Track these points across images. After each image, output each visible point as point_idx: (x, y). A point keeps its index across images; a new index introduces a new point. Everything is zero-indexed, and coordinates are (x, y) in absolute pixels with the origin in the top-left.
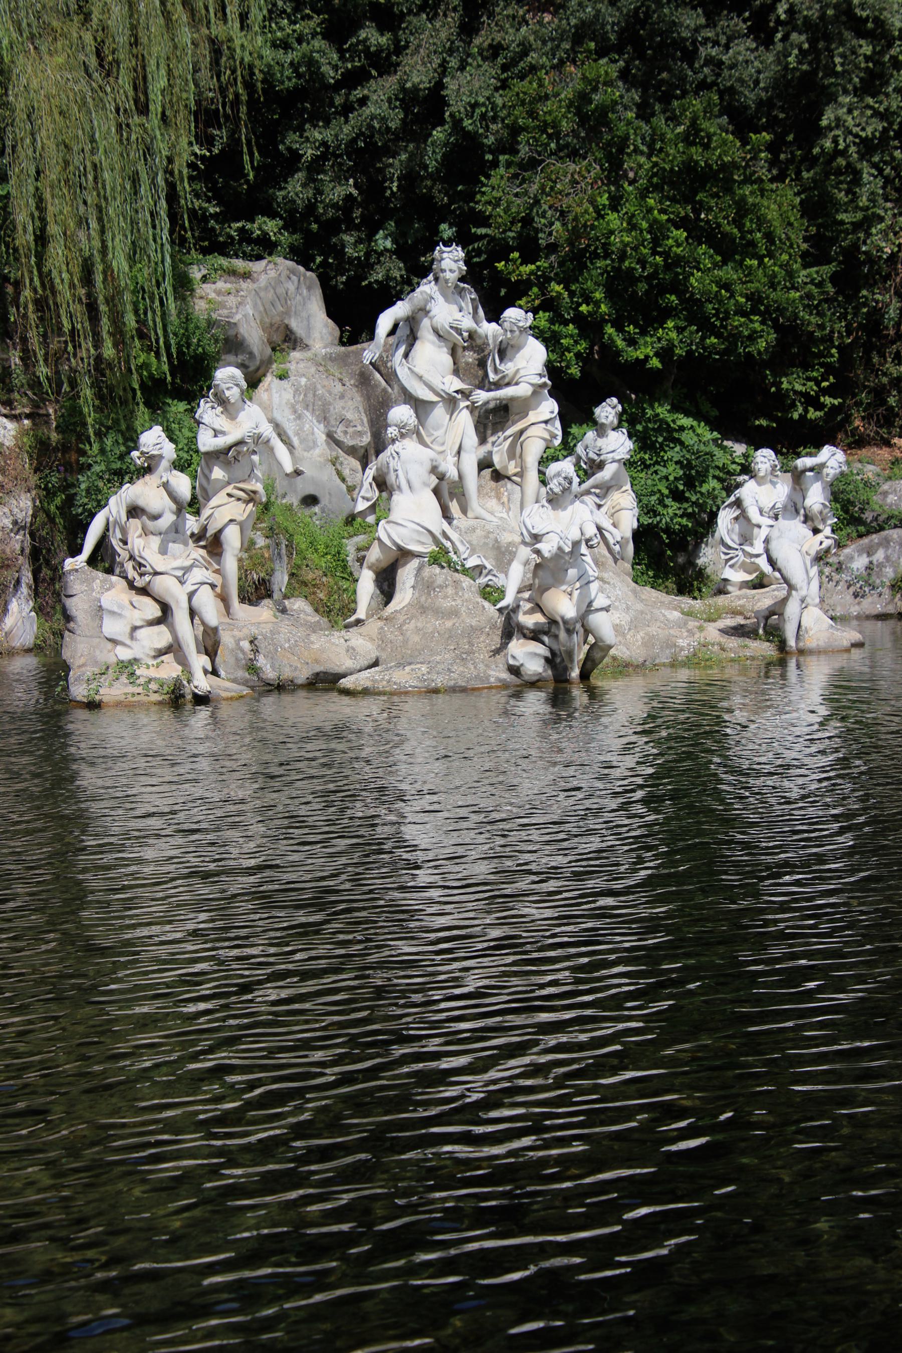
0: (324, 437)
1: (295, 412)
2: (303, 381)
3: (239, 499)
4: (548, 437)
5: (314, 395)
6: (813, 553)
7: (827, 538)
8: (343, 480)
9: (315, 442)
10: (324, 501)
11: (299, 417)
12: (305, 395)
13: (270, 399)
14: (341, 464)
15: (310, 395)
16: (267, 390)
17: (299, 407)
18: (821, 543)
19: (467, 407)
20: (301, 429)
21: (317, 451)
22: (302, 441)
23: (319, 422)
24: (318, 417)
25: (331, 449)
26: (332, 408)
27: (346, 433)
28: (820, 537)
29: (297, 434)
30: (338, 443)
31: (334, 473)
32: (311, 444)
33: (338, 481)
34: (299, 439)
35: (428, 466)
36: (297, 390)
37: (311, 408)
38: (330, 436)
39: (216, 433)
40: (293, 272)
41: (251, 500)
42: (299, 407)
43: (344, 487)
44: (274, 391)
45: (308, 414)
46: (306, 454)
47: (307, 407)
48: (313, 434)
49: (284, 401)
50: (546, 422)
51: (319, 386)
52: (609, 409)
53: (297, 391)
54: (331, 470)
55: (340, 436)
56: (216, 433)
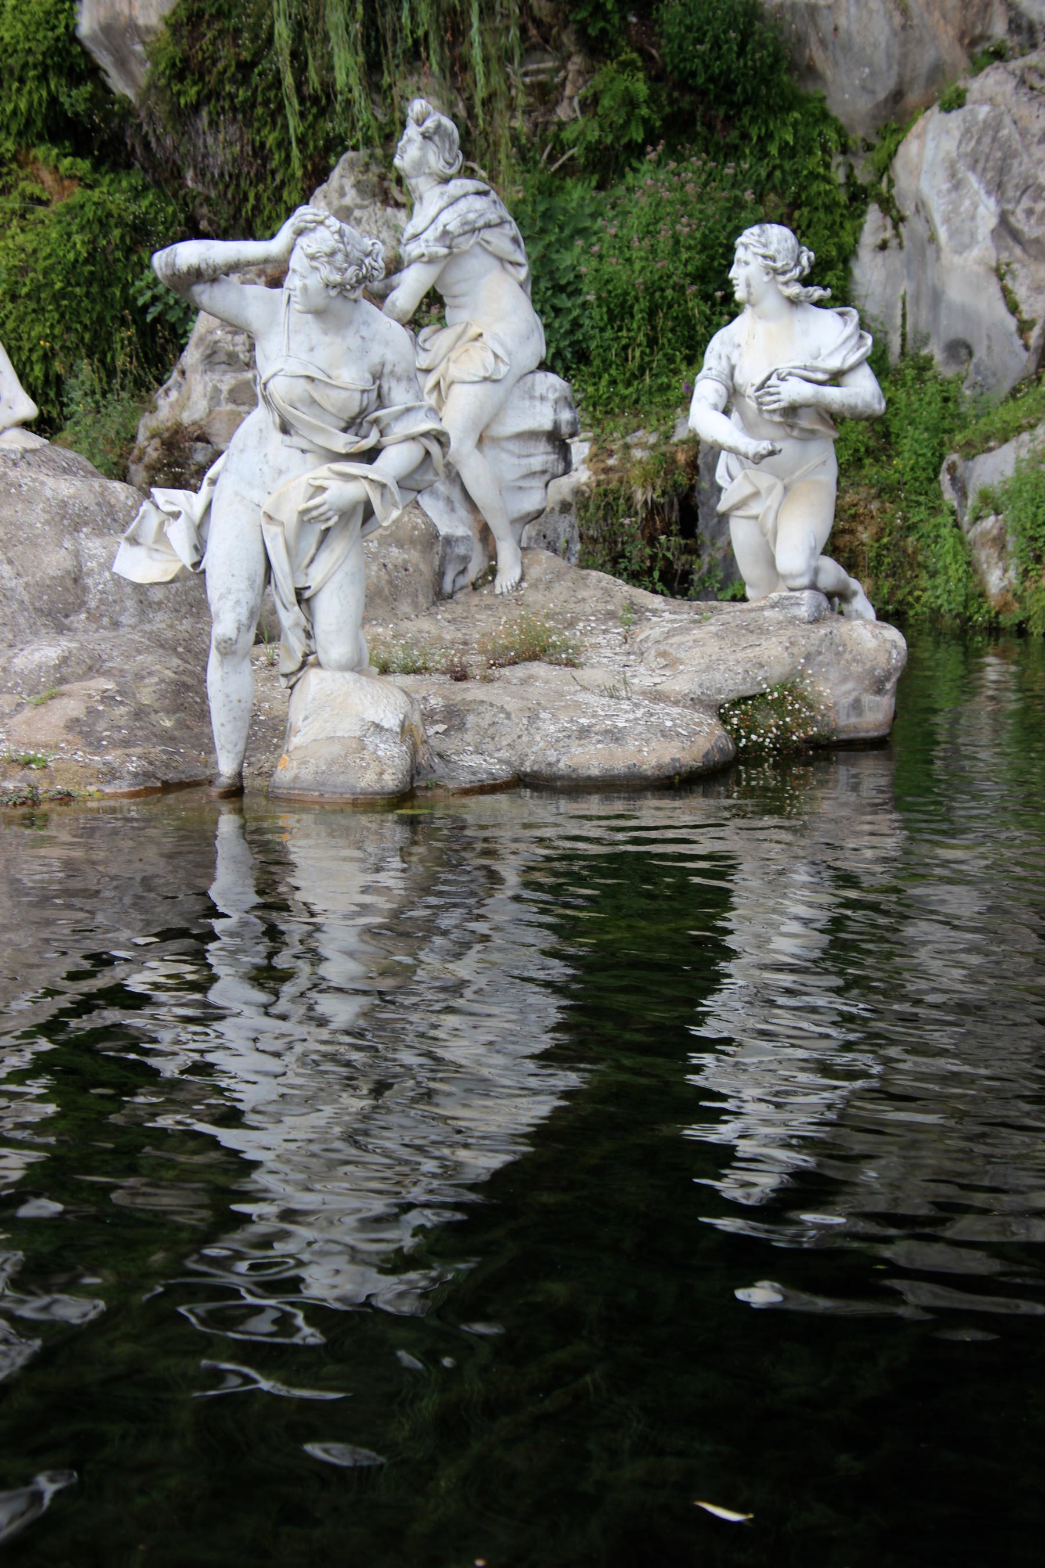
0: (993, 222)
1: (953, 175)
2: (983, 112)
5: (994, 139)
6: (289, 514)
8: (1013, 308)
9: (973, 235)
10: (980, 352)
11: (957, 185)
12: (979, 142)
13: (920, 154)
14: (1014, 278)
15: (987, 140)
16: (919, 136)
17: (962, 167)
18: (322, 489)
20: (955, 210)
21: (975, 253)
22: (952, 234)
23: (989, 193)
24: (988, 183)
25: (999, 249)
26: (1015, 163)
27: (1030, 212)
29: (947, 220)
30: (1015, 235)
31: (999, 294)
32: (966, 239)
33: (1001, 309)
34: (949, 229)
36: (968, 131)
37: (980, 166)
38: (1004, 219)
42: (962, 167)
43: (1012, 323)
44: (930, 136)
45: (973, 181)
46: (957, 260)
47: (973, 168)
48: (973, 218)
49: (941, 155)
51: (1007, 120)
54: (993, 289)
55: (1019, 220)
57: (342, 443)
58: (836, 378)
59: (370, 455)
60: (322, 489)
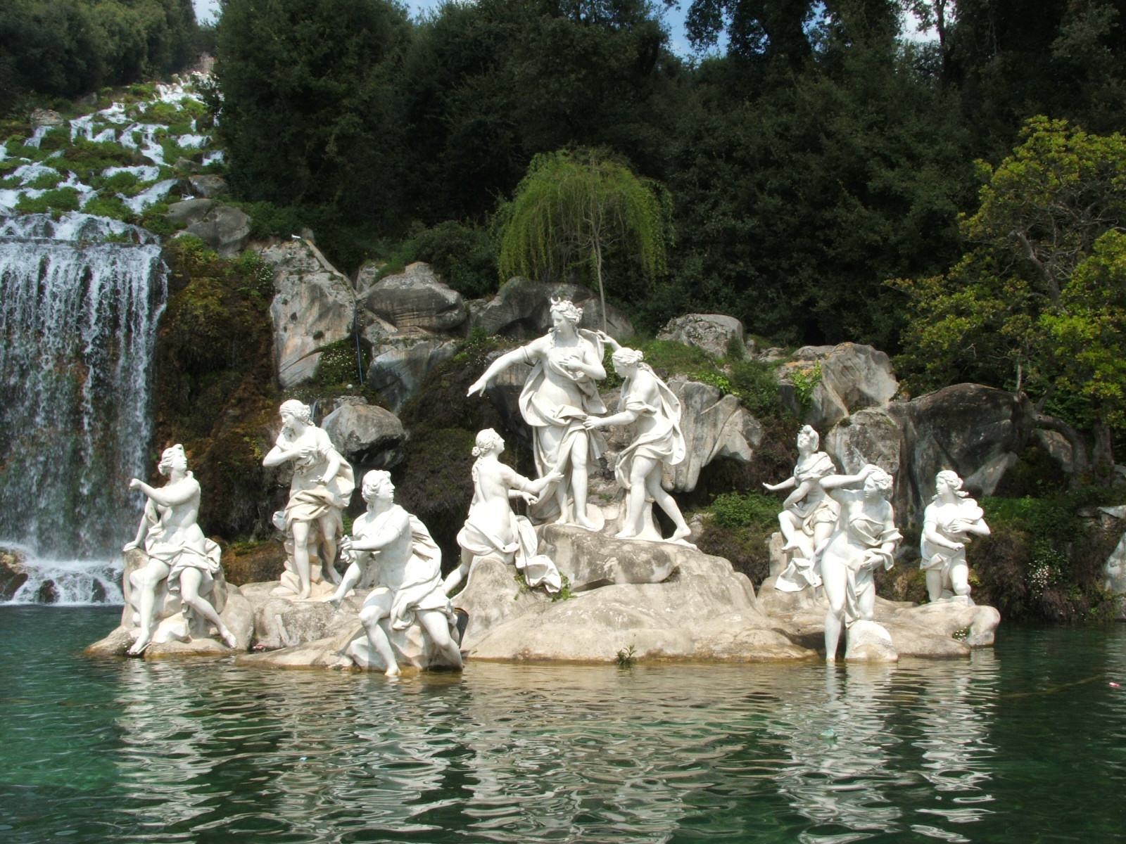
1: (849, 449)
3: (310, 503)
4: (653, 456)
6: (857, 567)
7: (878, 554)
11: (851, 453)
18: (869, 558)
19: (583, 430)
28: (869, 552)
35: (498, 478)
39: (283, 450)
40: (858, 351)
41: (325, 503)
50: (651, 443)
52: (804, 436)
53: (852, 436)
56: (283, 450)
57: (873, 542)
58: (974, 522)
59: (879, 546)
60: (869, 558)
